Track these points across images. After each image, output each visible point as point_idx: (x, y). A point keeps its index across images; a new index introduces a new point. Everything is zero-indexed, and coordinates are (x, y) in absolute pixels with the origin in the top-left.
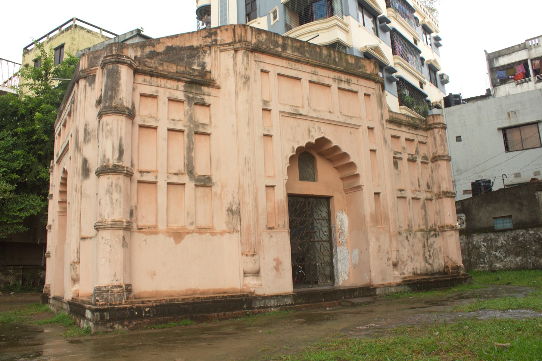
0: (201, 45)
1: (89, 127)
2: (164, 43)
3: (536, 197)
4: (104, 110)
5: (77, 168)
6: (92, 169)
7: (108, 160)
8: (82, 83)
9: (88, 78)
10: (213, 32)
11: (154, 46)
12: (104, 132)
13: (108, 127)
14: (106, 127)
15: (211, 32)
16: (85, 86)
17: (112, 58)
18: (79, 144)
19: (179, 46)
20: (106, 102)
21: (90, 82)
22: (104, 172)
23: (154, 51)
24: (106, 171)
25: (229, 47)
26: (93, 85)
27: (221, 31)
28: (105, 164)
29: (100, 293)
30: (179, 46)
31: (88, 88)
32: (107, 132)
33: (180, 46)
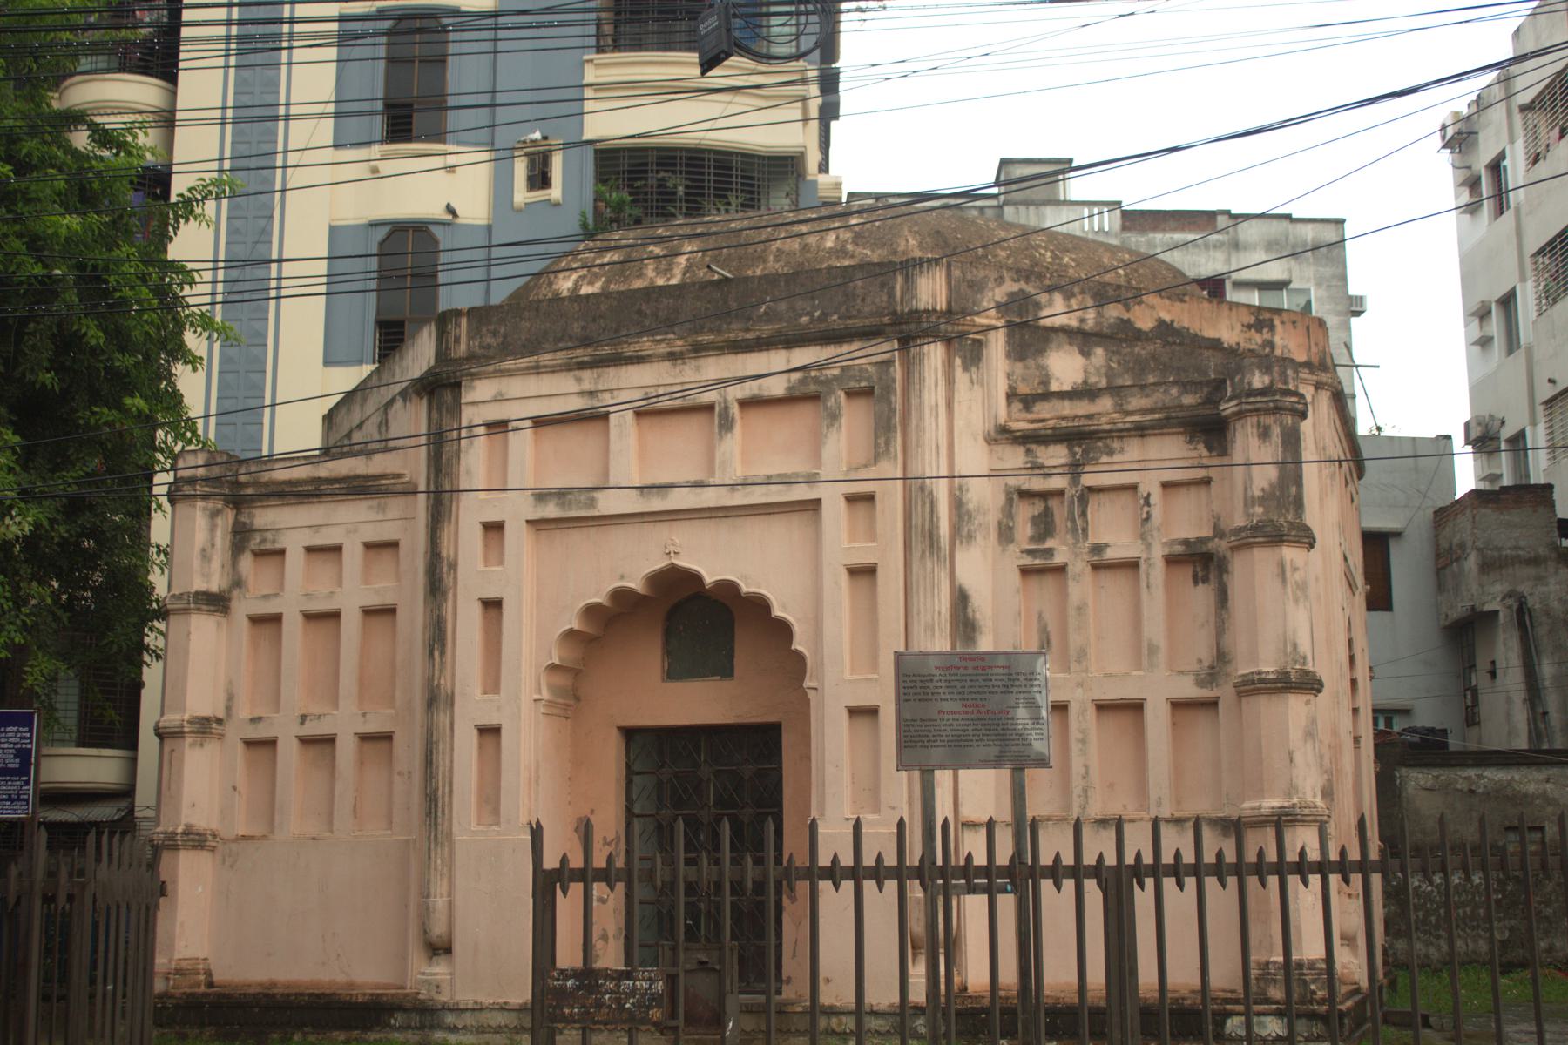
0: (1238, 344)
1: (969, 495)
2: (1152, 307)
3: (1395, 781)
4: (1293, 533)
5: (939, 613)
6: (982, 623)
7: (1304, 658)
8: (934, 354)
9: (960, 344)
10: (1265, 320)
11: (1128, 309)
12: (1289, 586)
13: (1297, 576)
14: (1292, 575)
15: (1261, 318)
16: (949, 365)
17: (1299, 403)
18: (942, 540)
19: (1188, 329)
20: (1288, 511)
21: (965, 357)
22: (1304, 686)
23: (1129, 320)
24: (1309, 686)
25: (1310, 377)
26: (974, 369)
27: (1283, 323)
28: (1298, 667)
29: (1316, 974)
30: (1188, 329)
31: (961, 377)
32: (1295, 587)
33: (1191, 331)
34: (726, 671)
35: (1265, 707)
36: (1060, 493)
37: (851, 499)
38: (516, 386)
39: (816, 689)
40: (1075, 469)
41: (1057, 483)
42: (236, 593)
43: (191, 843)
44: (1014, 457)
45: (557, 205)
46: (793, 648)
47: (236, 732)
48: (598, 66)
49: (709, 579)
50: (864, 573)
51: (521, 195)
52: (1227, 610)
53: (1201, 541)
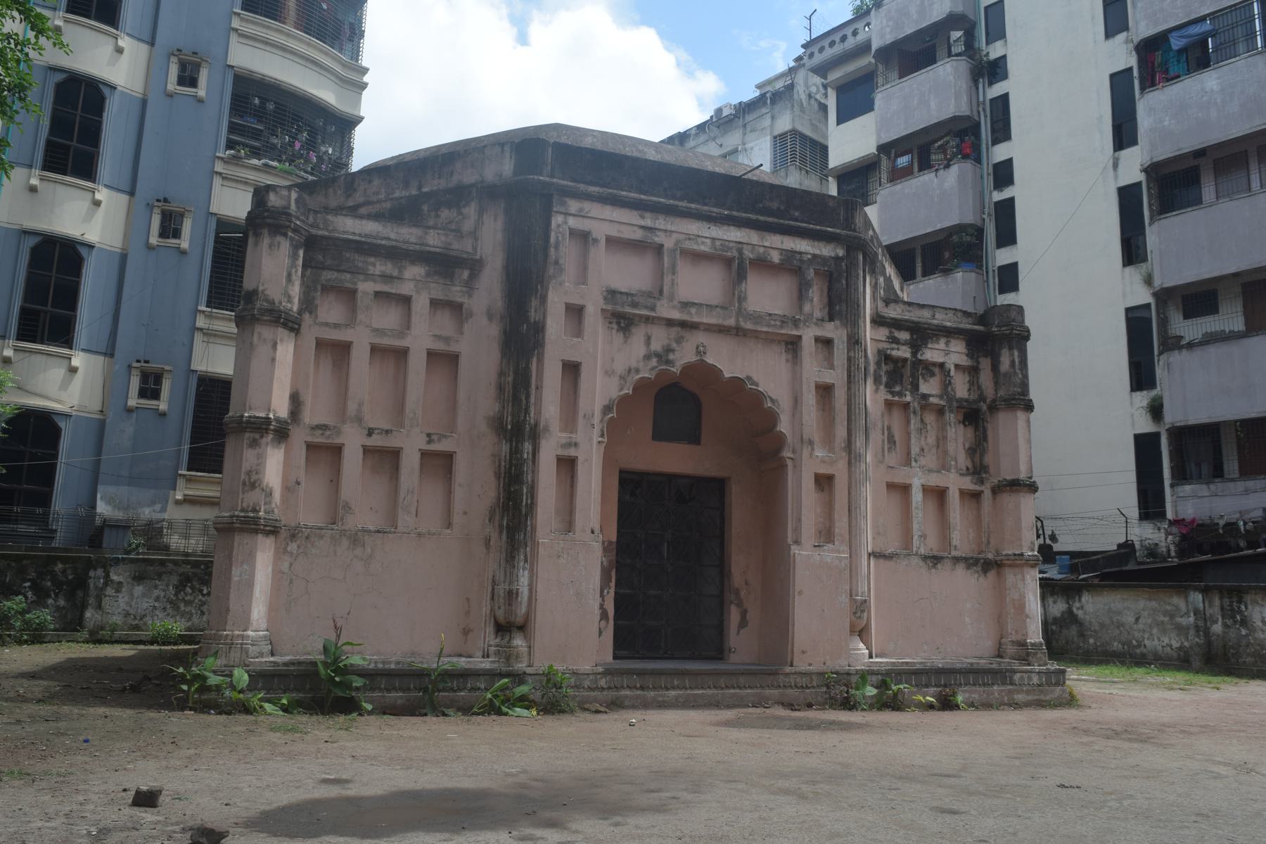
34: (693, 437)
35: (1008, 499)
36: (905, 360)
37: (818, 340)
38: (595, 209)
39: (792, 459)
40: (916, 347)
41: (904, 352)
42: (306, 316)
43: (268, 528)
44: (883, 333)
45: (200, 101)
46: (778, 429)
47: (299, 437)
48: (242, 19)
49: (727, 375)
50: (825, 391)
51: (172, 85)
52: (987, 442)
53: (975, 402)
